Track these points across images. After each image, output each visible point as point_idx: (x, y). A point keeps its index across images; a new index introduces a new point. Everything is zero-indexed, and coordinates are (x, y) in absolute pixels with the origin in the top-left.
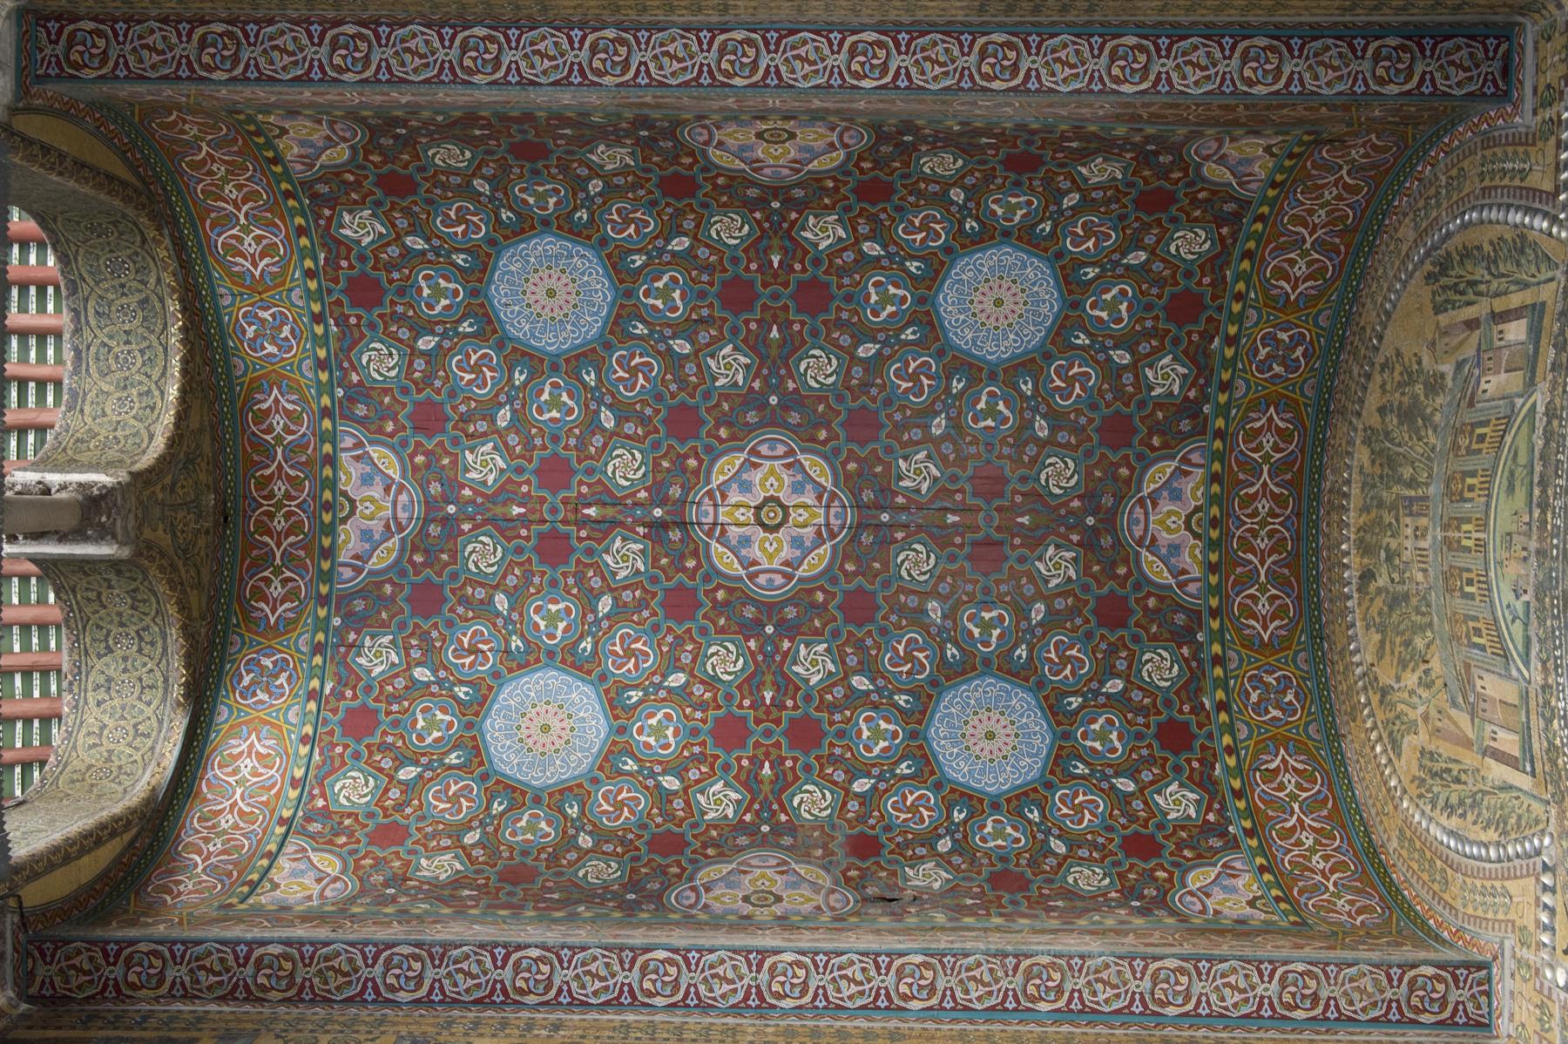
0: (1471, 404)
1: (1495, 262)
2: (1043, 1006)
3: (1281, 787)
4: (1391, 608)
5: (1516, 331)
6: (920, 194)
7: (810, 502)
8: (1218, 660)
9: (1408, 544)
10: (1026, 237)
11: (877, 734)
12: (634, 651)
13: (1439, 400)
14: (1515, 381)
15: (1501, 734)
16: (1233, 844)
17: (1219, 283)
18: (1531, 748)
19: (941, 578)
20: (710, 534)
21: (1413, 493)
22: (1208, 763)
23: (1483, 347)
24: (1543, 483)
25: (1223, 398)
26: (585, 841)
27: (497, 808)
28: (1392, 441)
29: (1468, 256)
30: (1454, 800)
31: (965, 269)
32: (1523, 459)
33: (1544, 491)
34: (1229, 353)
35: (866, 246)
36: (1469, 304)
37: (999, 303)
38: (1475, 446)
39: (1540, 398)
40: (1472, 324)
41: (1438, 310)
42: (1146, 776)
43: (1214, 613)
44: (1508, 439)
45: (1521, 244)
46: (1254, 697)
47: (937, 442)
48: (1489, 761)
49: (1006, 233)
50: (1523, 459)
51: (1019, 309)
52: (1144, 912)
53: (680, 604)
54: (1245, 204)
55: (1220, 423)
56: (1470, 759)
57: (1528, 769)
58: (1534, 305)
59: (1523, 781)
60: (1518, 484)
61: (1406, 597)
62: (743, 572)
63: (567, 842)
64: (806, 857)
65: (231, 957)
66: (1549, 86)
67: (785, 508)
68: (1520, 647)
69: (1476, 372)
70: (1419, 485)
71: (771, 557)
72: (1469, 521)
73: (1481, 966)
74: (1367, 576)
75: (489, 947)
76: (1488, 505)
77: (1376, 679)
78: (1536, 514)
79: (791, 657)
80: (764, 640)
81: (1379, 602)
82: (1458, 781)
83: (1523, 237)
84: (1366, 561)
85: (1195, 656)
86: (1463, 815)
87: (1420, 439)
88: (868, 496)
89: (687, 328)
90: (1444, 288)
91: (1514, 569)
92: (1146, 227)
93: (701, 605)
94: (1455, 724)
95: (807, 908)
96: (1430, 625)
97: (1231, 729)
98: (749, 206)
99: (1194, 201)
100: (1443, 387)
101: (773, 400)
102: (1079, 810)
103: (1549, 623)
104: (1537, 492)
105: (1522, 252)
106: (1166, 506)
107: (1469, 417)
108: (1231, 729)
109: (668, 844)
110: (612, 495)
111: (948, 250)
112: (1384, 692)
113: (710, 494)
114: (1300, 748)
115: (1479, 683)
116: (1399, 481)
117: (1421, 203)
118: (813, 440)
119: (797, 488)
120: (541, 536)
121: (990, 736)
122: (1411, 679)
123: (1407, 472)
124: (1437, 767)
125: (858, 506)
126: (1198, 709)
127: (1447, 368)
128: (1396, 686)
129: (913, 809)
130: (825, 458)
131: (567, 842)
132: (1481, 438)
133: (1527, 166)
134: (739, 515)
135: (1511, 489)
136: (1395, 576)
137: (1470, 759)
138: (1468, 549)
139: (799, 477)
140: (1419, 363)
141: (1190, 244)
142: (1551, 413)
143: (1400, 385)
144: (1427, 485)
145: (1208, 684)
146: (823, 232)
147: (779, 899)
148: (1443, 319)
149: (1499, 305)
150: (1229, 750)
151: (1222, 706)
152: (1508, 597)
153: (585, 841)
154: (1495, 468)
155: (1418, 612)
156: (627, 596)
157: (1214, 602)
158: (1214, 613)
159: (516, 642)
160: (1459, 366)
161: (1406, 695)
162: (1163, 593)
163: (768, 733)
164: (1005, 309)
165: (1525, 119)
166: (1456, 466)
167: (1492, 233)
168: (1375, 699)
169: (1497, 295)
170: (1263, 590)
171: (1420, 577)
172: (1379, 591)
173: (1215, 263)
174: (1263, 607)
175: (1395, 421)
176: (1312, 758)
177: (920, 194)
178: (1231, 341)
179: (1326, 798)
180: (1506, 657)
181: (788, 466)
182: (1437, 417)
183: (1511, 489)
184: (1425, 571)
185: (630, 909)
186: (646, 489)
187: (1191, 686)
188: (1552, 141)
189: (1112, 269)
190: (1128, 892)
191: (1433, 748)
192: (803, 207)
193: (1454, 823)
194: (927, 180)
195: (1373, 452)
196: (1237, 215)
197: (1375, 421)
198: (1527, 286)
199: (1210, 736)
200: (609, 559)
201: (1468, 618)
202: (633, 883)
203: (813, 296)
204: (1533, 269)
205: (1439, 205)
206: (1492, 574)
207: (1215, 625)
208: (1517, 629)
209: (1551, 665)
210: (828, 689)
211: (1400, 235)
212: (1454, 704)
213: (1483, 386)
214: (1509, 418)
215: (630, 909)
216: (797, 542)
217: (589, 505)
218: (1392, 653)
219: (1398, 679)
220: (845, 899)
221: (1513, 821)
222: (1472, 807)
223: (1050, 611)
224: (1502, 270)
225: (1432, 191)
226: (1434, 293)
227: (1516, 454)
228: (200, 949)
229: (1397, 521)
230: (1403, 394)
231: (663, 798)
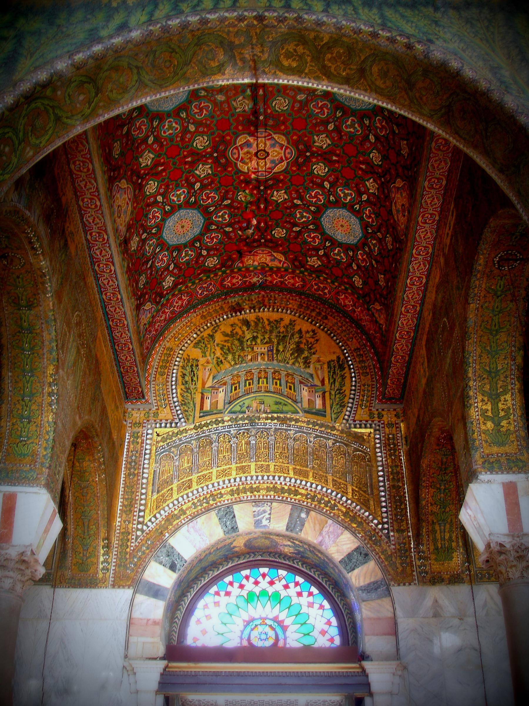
0: (301, 383)
1: (339, 393)
3: (177, 303)
4: (239, 340)
5: (319, 403)
7: (267, 166)
8: (216, 275)
9: (259, 350)
13: (302, 364)
14: (305, 405)
15: (209, 401)
16: (157, 303)
18: (207, 415)
21: (275, 352)
22: (181, 284)
23: (316, 388)
24: (278, 418)
25: (306, 274)
28: (290, 339)
29: (343, 379)
30: (187, 378)
32: (285, 408)
33: (276, 418)
34: (321, 278)
36: (329, 380)
38: (288, 384)
39: (301, 416)
40: (323, 382)
41: (329, 363)
44: (290, 401)
45: (342, 406)
46: (204, 286)
48: (200, 395)
50: (285, 408)
53: (223, 124)
55: (298, 272)
56: (199, 385)
57: (202, 414)
58: (325, 412)
59: (197, 415)
60: (277, 406)
61: (243, 349)
62: (238, 145)
65: (84, 153)
66: (383, 416)
67: (265, 158)
68: (233, 410)
69: (309, 385)
70: (277, 355)
72: (267, 383)
73: (143, 397)
74: (247, 323)
75: (97, 190)
76: (271, 392)
77: (216, 331)
78: (270, 416)
79: (205, 163)
80: (211, 154)
81: (240, 333)
82: (192, 380)
83: (344, 406)
84: (253, 324)
86: (183, 384)
87: (291, 355)
89: (338, 129)
90: (335, 367)
91: (254, 405)
93: (223, 132)
94: (208, 378)
96: (236, 364)
100: (306, 367)
103: (241, 422)
104: (275, 415)
105: (341, 406)
106: (268, 258)
107: (297, 382)
108: (194, 283)
110: (268, 100)
112: (212, 336)
113: (270, 135)
114: (189, 302)
115: (221, 390)
116: (278, 344)
117: (362, 353)
122: (218, 353)
123: (281, 348)
124: (194, 369)
125: (266, 180)
126: (199, 274)
127: (311, 370)
128: (215, 344)
130: (285, 169)
132: (290, 389)
133: (363, 407)
135: (277, 403)
136: (249, 343)
137: (199, 385)
138: (259, 383)
139: (277, 162)
140: (314, 354)
142: (297, 421)
143: (307, 341)
144: (277, 360)
145: (208, 274)
148: (326, 366)
149: (327, 394)
150: (187, 287)
151: (201, 280)
152: (247, 403)
154: (282, 395)
155: (239, 356)
157: (236, 270)
158: (232, 271)
160: (311, 375)
161: (213, 350)
163: (174, 164)
165: (377, 405)
166: (283, 373)
167: (347, 393)
168: (209, 331)
169: (330, 393)
170: (240, 280)
171: (249, 357)
172: (243, 332)
173: (352, 285)
174: (234, 281)
175: (297, 340)
176: (187, 305)
178: (326, 279)
179: (174, 313)
180: (230, 403)
181: (282, 158)
182: (297, 365)
183: (277, 403)
184: (251, 360)
186: (271, 112)
187: (207, 271)
188: (368, 418)
191: (200, 366)
193: (180, 379)
195: (287, 326)
197: (297, 328)
198: (331, 408)
199: (190, 280)
200: (241, 98)
201: (239, 382)
204: (335, 411)
205: (360, 362)
206: (253, 395)
207: (228, 272)
208: (238, 408)
209: (230, 423)
211: (354, 340)
212: (214, 378)
213: (306, 388)
214: (295, 402)
217: (264, 91)
218: (225, 341)
219: (218, 345)
221: (186, 408)
222: (186, 388)
224: (337, 396)
225: (364, 358)
226: (334, 361)
227: (286, 405)
228: (85, 143)
229: (266, 343)
230: (305, 345)
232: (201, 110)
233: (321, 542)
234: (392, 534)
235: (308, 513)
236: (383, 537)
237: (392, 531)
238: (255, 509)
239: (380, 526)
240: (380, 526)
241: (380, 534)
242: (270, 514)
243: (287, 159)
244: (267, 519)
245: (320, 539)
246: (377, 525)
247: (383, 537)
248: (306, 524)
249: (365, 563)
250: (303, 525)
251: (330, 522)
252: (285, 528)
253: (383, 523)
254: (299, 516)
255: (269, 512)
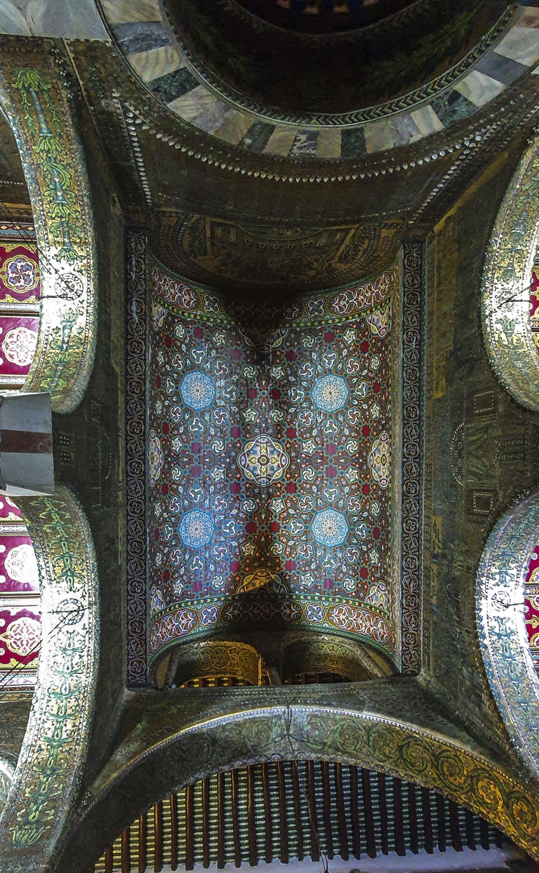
2: (418, 375)
6: (166, 414)
10: (177, 382)
11: (331, 427)
12: (306, 502)
17: (192, 323)
19: (282, 408)
20: (270, 479)
26: (365, 514)
27: (355, 541)
31: (188, 401)
35: (181, 432)
37: (197, 391)
42: (342, 346)
43: (291, 326)
47: (240, 410)
49: (177, 388)
51: (199, 384)
52: (386, 347)
54: (169, 314)
63: (366, 519)
64: (370, 448)
67: (262, 456)
71: (277, 461)
85: (304, 331)
88: (257, 431)
92: (176, 345)
95: (387, 446)
97: (327, 322)
98: (170, 468)
99: (169, 330)
101: (228, 460)
102: (353, 366)
109: (366, 490)
111: (182, 406)
113: (257, 479)
118: (240, 448)
119: (255, 453)
120: (271, 532)
121: (330, 393)
126: (321, 330)
129: (354, 416)
131: (366, 519)
134: (264, 470)
141: (180, 331)
146: (177, 445)
147: (384, 455)
153: (365, 514)
156: (289, 505)
159: (303, 538)
162: (285, 340)
163: (331, 461)
164: (199, 388)
173: (185, 324)
177: (166, 414)
185: (388, 499)
189: (186, 356)
190: (379, 351)
192: (170, 451)
194: (162, 412)
196: (172, 316)
202: (379, 499)
203: (196, 448)
210: (317, 443)
215: (388, 499)
216: (272, 453)
220: (384, 435)
223: (291, 375)
231: (352, 492)
232: (307, 504)
233: (226, 111)
234: (118, 111)
235: (242, 143)
236: (132, 108)
237: (118, 115)
238: (313, 152)
239: (138, 122)
240: (138, 122)
241: (137, 112)
242: (295, 145)
243: (244, 455)
244: (299, 140)
245: (227, 114)
246: (143, 123)
247: (132, 108)
248: (245, 131)
249: (158, 79)
250: (250, 132)
251: (211, 133)
252: (276, 130)
253: (134, 124)
254: (254, 141)
255: (295, 147)
